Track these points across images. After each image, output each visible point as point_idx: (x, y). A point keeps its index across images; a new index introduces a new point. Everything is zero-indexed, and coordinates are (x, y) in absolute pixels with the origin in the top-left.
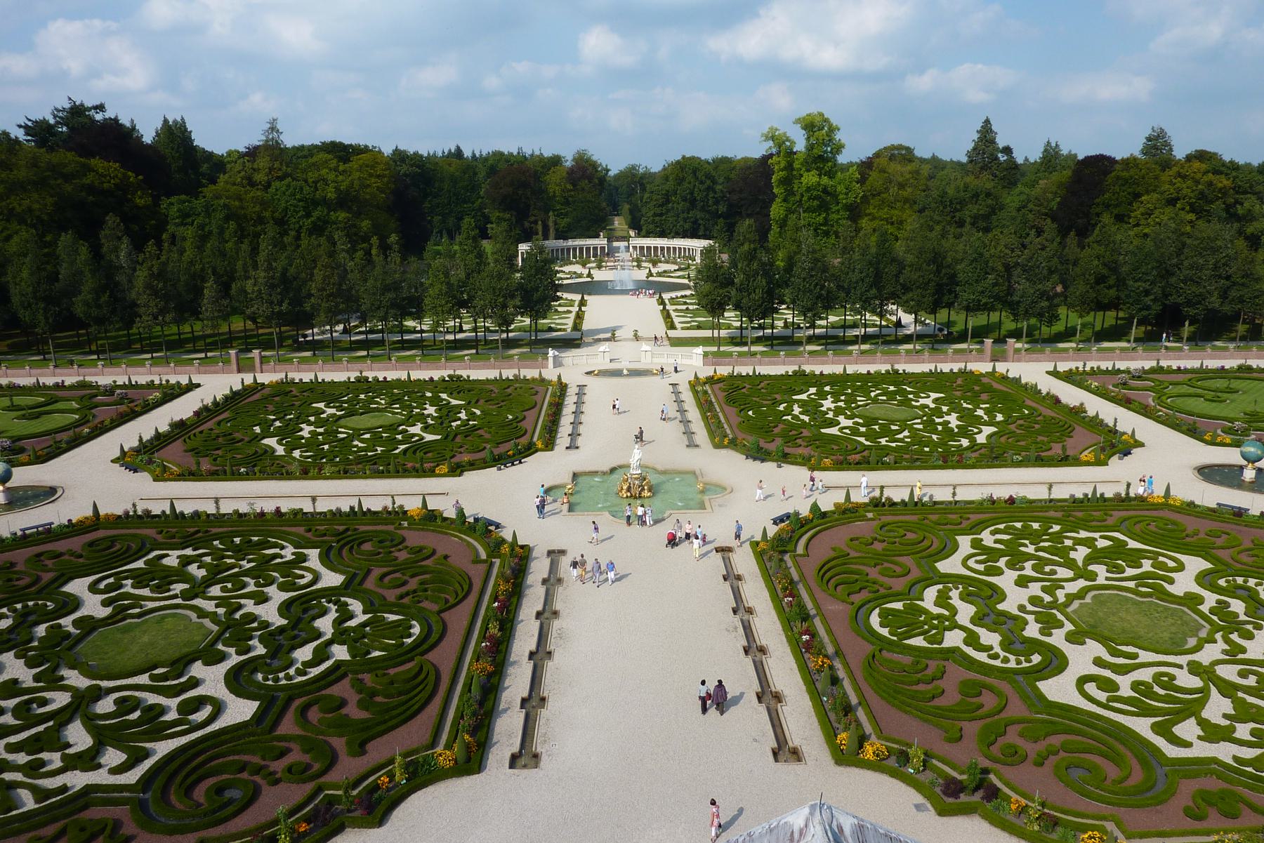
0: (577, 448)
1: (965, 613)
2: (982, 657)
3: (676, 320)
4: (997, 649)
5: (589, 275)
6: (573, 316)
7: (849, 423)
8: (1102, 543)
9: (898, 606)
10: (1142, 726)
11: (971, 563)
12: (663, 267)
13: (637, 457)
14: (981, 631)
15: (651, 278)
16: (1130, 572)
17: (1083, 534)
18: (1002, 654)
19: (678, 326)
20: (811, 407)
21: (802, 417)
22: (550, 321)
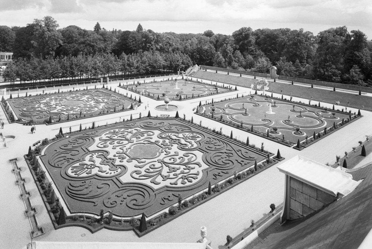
1: (98, 161)
2: (104, 174)
4: (108, 171)
7: (60, 108)
8: (134, 132)
9: (77, 164)
10: (147, 182)
11: (99, 145)
14: (103, 166)
16: (142, 138)
17: (130, 130)
18: (110, 172)
20: (47, 104)
21: (44, 108)
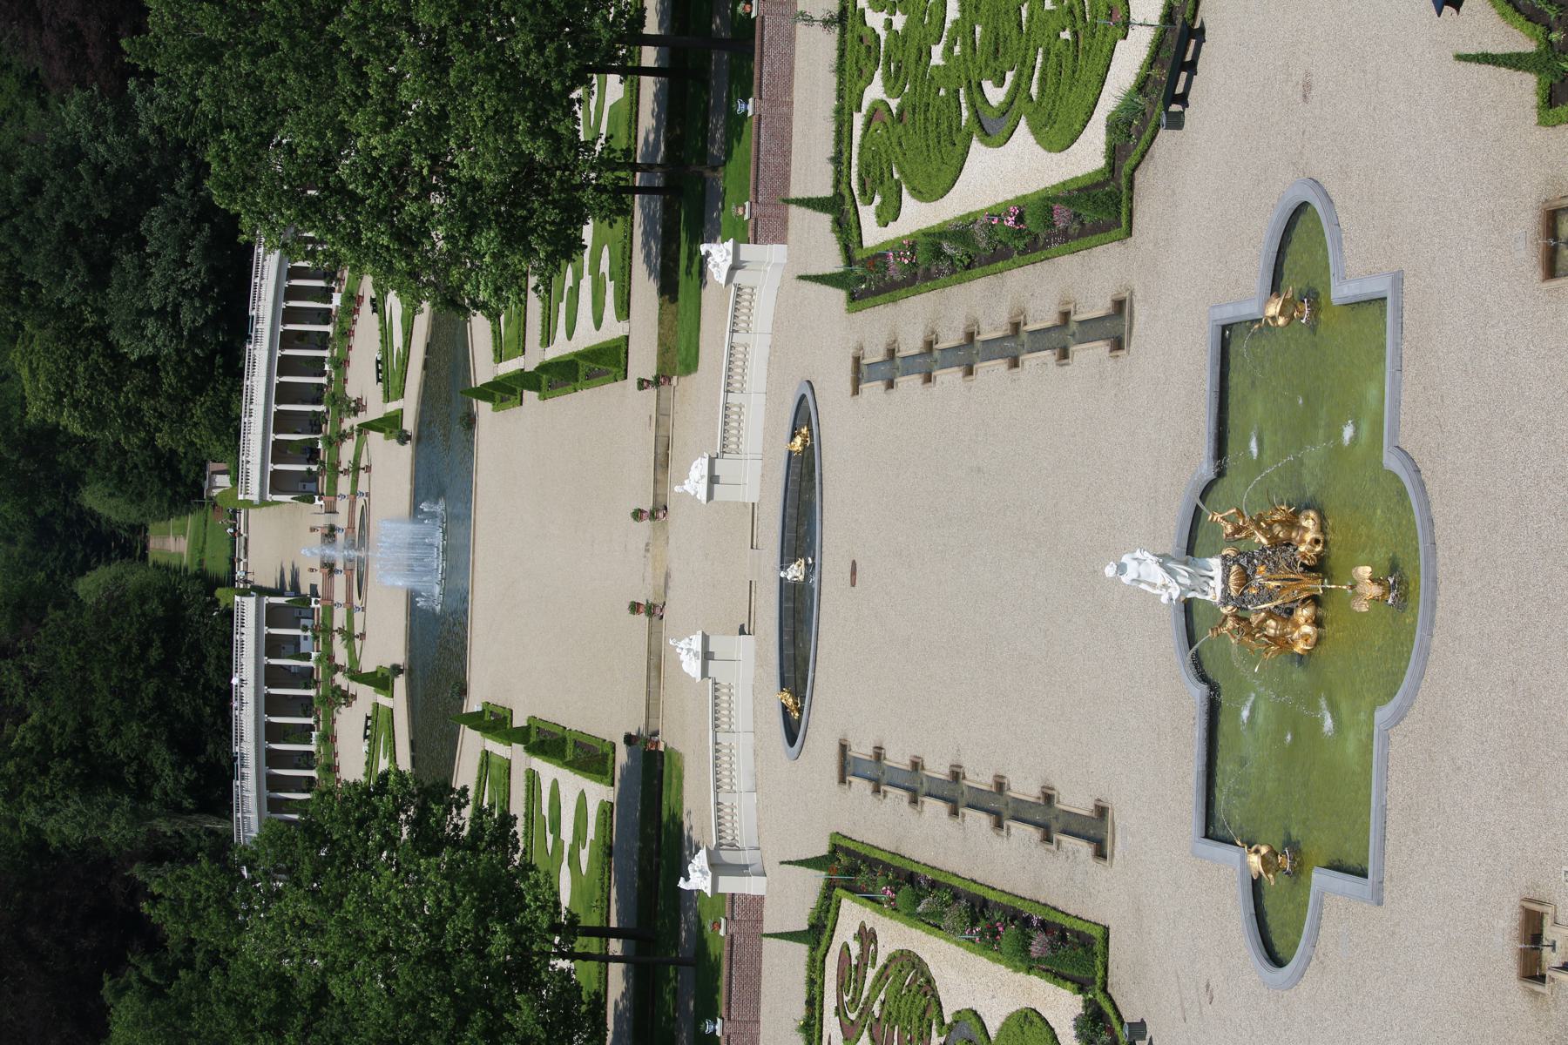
0: (1102, 811)
3: (587, 336)
5: (381, 681)
6: (548, 771)
12: (361, 381)
13: (1157, 575)
15: (409, 424)
19: (613, 328)
22: (565, 868)
